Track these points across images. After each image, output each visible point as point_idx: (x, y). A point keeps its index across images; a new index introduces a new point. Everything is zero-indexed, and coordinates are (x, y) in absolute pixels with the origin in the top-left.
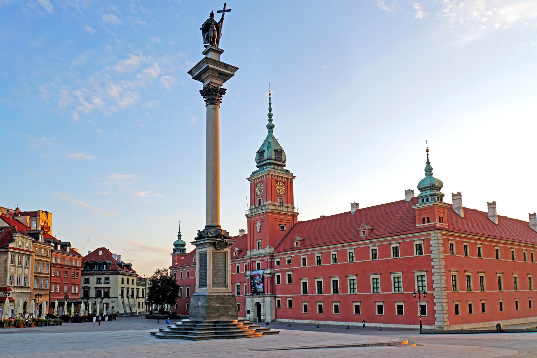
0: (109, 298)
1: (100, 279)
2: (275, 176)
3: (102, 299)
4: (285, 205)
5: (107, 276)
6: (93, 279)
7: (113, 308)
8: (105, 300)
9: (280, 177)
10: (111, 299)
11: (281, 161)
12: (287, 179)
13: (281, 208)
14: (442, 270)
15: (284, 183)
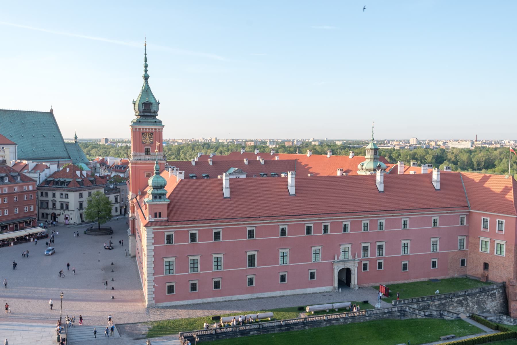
0: (69, 210)
1: (62, 194)
2: (140, 129)
3: (64, 211)
4: (151, 154)
5: (67, 193)
6: (58, 194)
7: (71, 219)
8: (66, 212)
9: (146, 129)
10: (70, 212)
11: (151, 112)
12: (155, 129)
13: (148, 157)
14: (150, 260)
15: (152, 134)
